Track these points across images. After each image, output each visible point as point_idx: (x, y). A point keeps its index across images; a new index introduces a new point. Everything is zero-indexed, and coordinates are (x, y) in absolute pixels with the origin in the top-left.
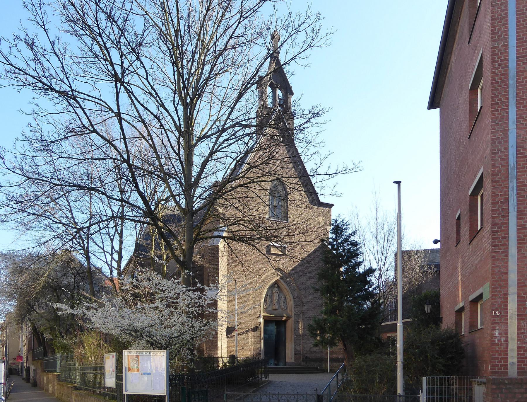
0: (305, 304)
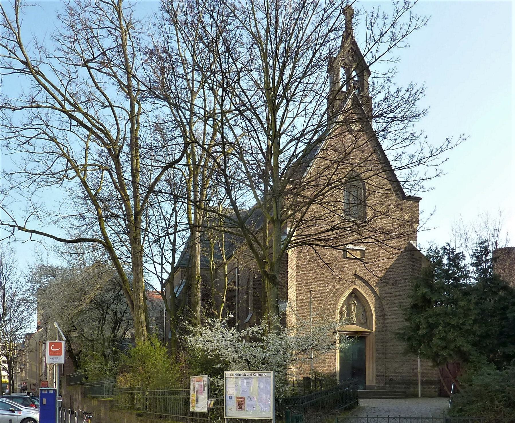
0: (388, 317)
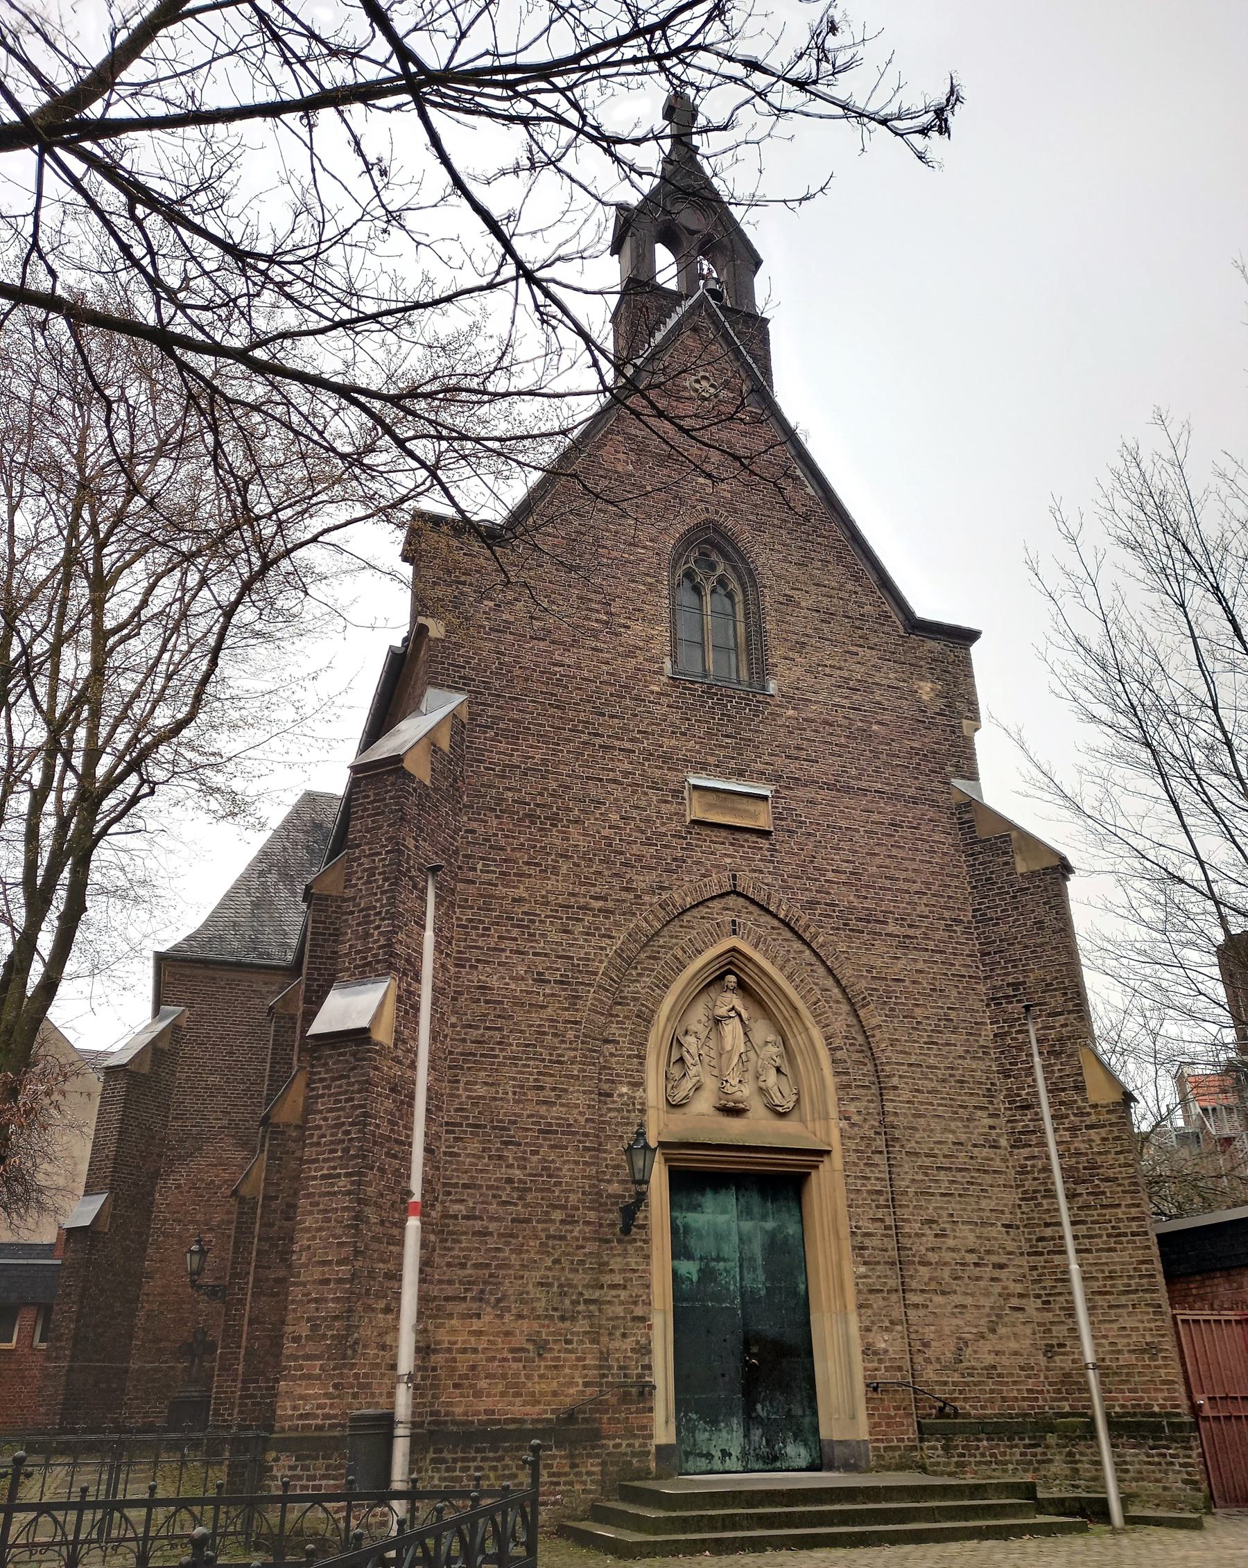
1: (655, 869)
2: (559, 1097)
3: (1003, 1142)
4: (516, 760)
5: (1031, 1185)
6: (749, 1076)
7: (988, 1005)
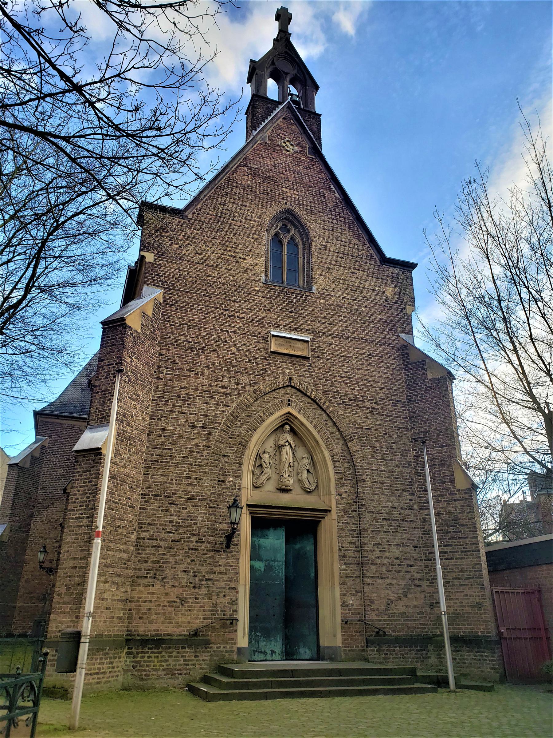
0: (364, 477)
1: (252, 374)
2: (199, 482)
3: (416, 507)
4: (185, 321)
5: (428, 527)
6: (294, 473)
7: (412, 442)
